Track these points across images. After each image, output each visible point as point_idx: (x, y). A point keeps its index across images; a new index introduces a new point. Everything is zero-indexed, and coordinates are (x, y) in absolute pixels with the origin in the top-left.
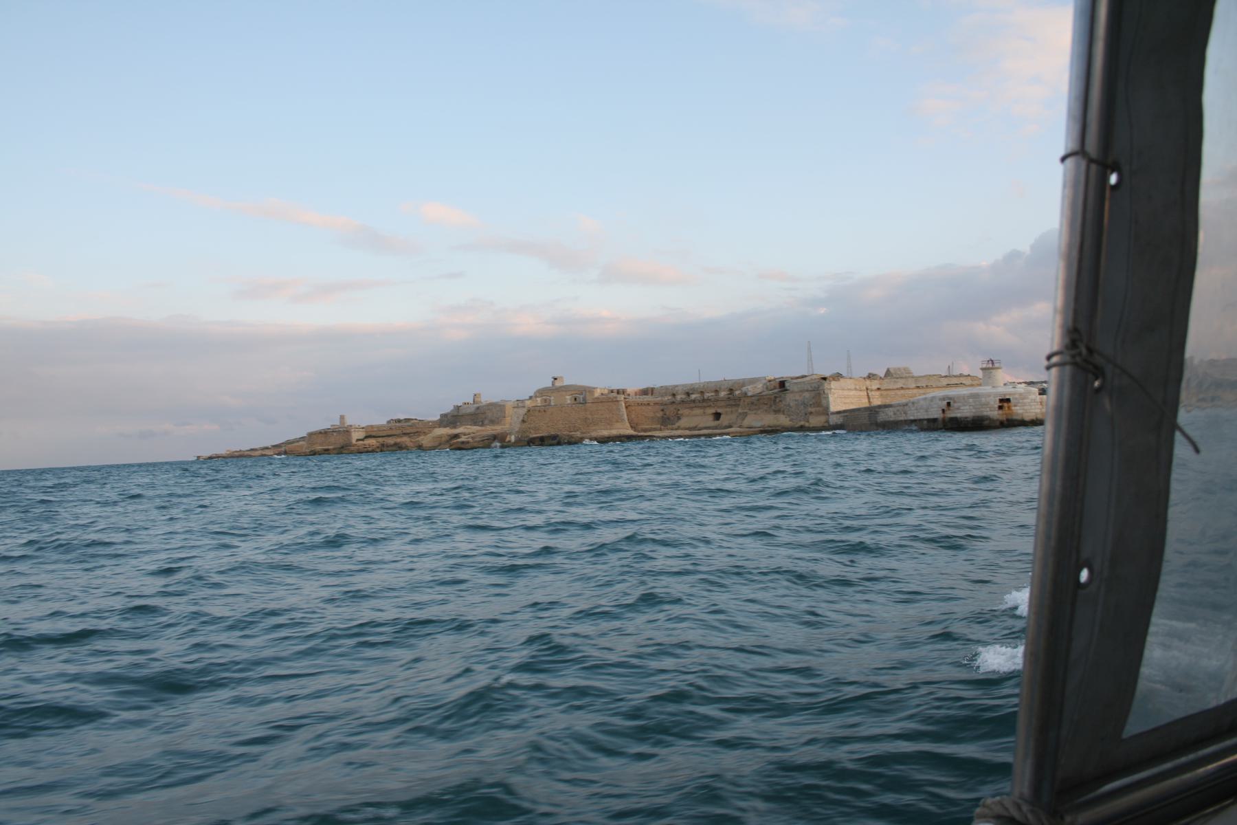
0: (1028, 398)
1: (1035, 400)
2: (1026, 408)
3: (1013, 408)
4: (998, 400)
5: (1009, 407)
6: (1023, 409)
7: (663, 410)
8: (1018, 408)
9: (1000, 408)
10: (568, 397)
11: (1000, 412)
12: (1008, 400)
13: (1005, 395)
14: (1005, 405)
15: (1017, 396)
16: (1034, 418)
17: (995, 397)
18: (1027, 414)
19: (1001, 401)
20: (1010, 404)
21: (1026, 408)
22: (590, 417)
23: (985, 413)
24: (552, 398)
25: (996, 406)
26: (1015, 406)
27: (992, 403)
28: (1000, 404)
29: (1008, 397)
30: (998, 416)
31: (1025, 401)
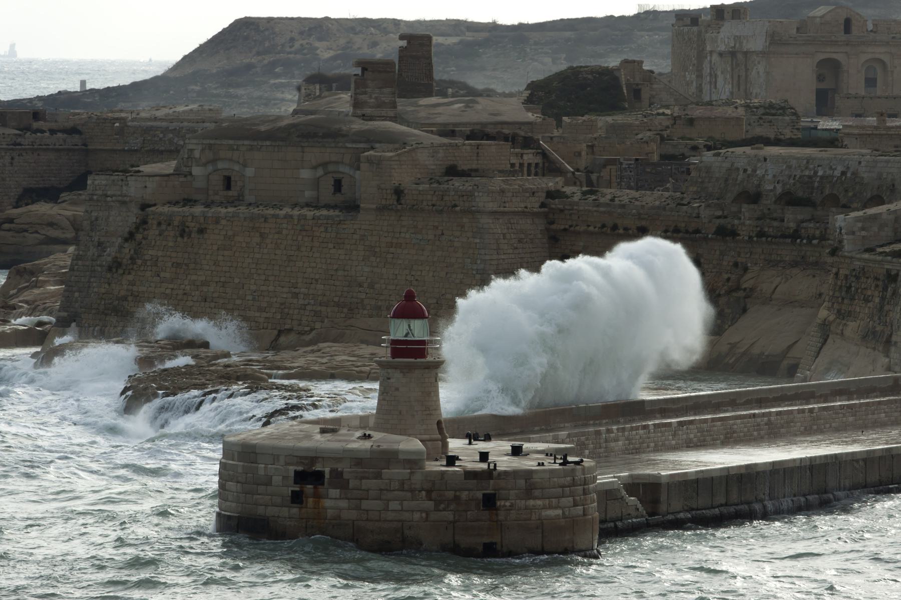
0: (378, 476)
1: (402, 483)
4: (292, 474)
6: (358, 508)
9: (297, 498)
10: (306, 174)
11: (295, 511)
12: (318, 477)
13: (313, 460)
15: (345, 467)
17: (287, 464)
21: (365, 504)
23: (261, 510)
24: (250, 172)
27: (277, 480)
28: (297, 488)
29: (318, 467)
31: (366, 484)
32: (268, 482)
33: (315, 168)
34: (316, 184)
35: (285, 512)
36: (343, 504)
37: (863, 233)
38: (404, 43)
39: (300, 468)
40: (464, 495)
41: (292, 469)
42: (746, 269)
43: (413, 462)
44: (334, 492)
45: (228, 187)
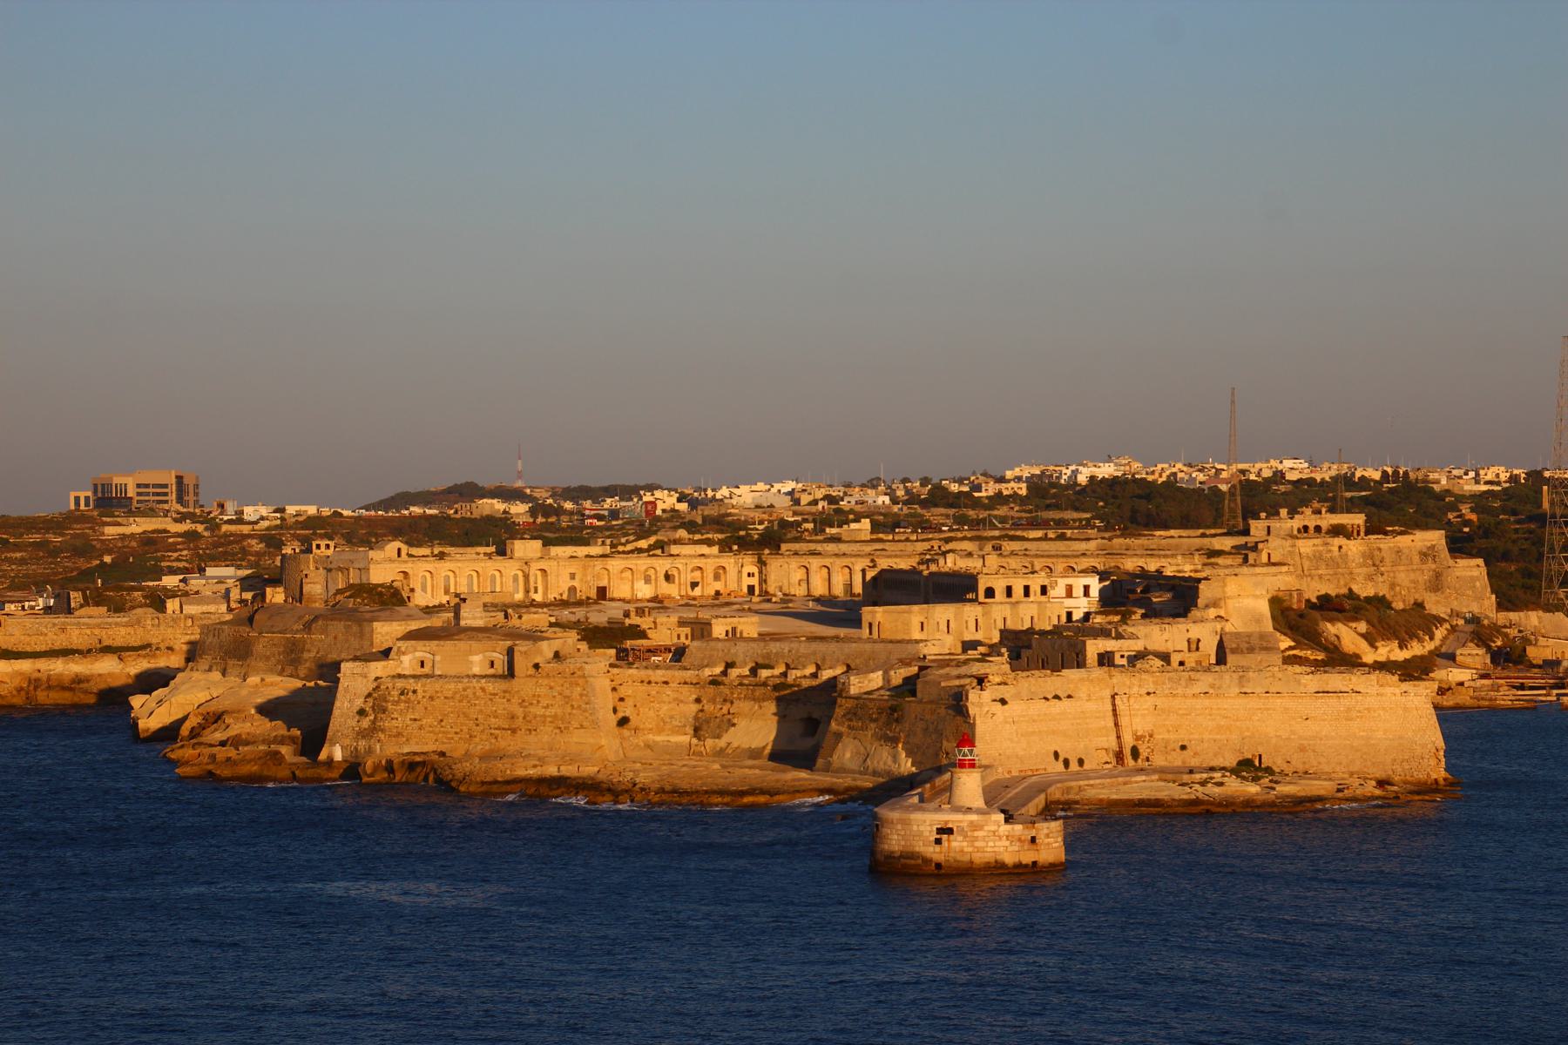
2: (977, 844)
6: (973, 846)
7: (698, 701)
11: (938, 848)
12: (950, 831)
14: (945, 837)
18: (979, 855)
19: (941, 831)
21: (977, 844)
22: (519, 712)
23: (917, 849)
25: (933, 839)
28: (938, 836)
29: (950, 826)
35: (931, 849)
36: (965, 844)
40: (1023, 838)
44: (960, 838)
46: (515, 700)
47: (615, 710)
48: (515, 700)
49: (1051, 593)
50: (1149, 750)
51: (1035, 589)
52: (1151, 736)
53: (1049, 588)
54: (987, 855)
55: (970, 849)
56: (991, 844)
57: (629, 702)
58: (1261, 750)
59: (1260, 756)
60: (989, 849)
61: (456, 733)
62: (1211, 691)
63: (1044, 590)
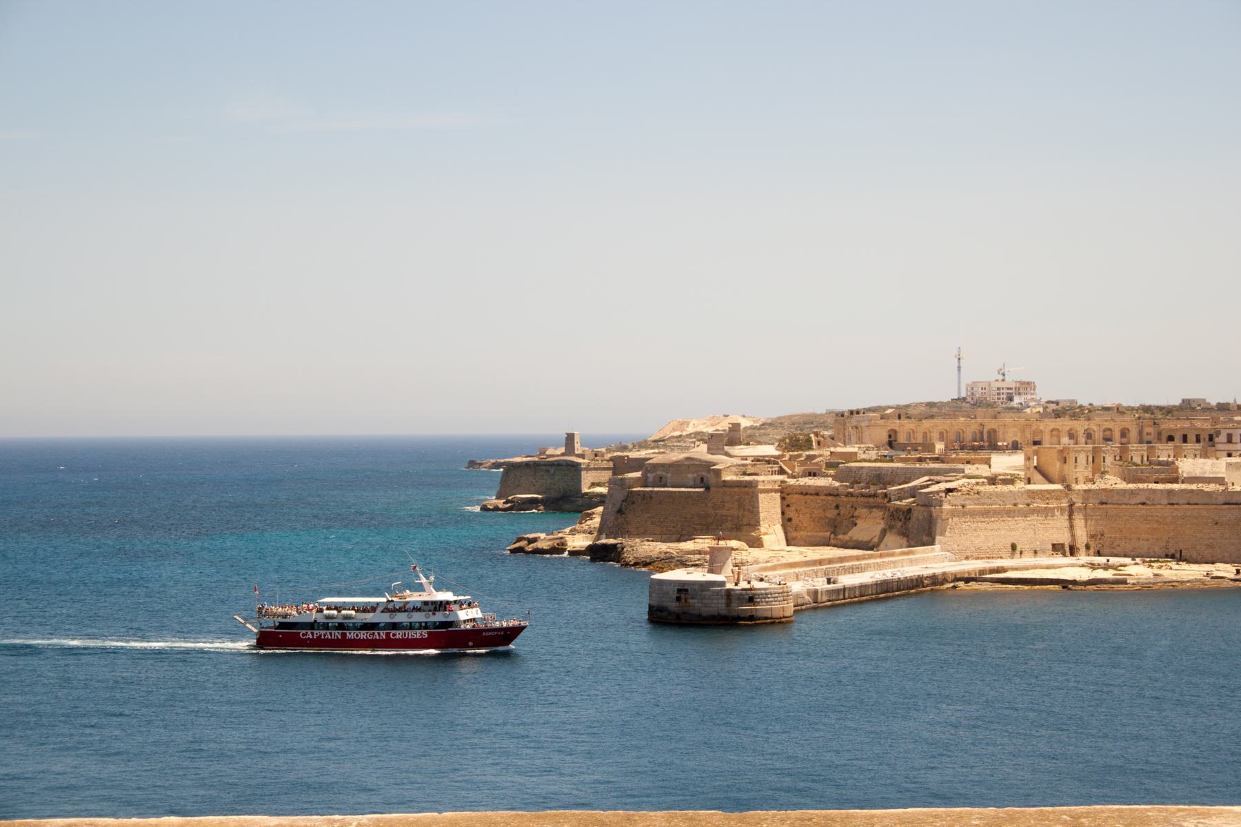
2: (704, 601)
3: (691, 601)
5: (686, 600)
6: (702, 603)
7: (837, 507)
8: (695, 601)
9: (678, 599)
11: (677, 604)
12: (686, 590)
15: (696, 587)
16: (716, 614)
17: (674, 586)
18: (706, 609)
19: (679, 590)
20: (687, 596)
21: (704, 601)
23: (665, 604)
25: (674, 597)
26: (693, 598)
27: (671, 592)
29: (686, 588)
30: (676, 609)
31: (704, 593)
32: (668, 594)
33: (693, 473)
34: (695, 479)
37: (899, 495)
38: (730, 426)
39: (679, 588)
41: (676, 588)
42: (856, 509)
43: (723, 584)
45: (661, 481)
46: (710, 505)
47: (783, 513)
48: (710, 505)
49: (1216, 440)
50: (1100, 545)
51: (1205, 436)
52: (1102, 535)
53: (1214, 436)
54: (711, 609)
55: (700, 605)
56: (715, 601)
57: (793, 508)
58: (1181, 546)
59: (1181, 551)
60: (714, 605)
61: (674, 527)
62: (1147, 502)
63: (1211, 438)
